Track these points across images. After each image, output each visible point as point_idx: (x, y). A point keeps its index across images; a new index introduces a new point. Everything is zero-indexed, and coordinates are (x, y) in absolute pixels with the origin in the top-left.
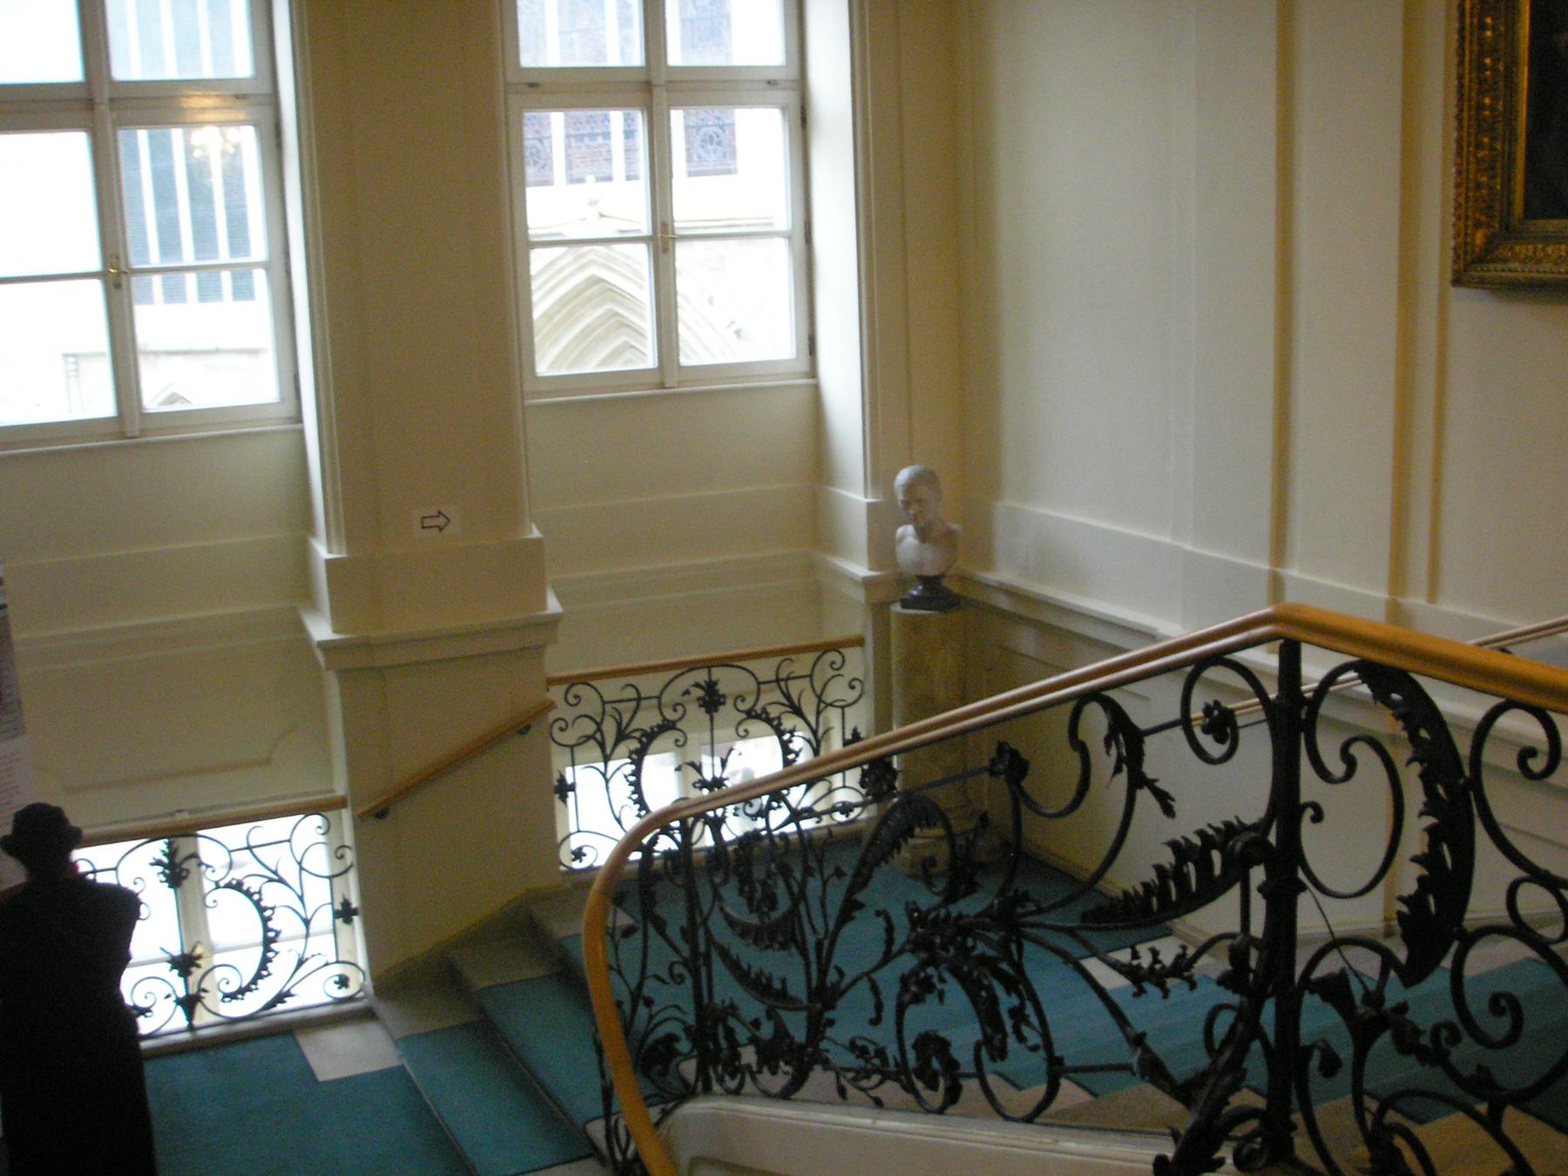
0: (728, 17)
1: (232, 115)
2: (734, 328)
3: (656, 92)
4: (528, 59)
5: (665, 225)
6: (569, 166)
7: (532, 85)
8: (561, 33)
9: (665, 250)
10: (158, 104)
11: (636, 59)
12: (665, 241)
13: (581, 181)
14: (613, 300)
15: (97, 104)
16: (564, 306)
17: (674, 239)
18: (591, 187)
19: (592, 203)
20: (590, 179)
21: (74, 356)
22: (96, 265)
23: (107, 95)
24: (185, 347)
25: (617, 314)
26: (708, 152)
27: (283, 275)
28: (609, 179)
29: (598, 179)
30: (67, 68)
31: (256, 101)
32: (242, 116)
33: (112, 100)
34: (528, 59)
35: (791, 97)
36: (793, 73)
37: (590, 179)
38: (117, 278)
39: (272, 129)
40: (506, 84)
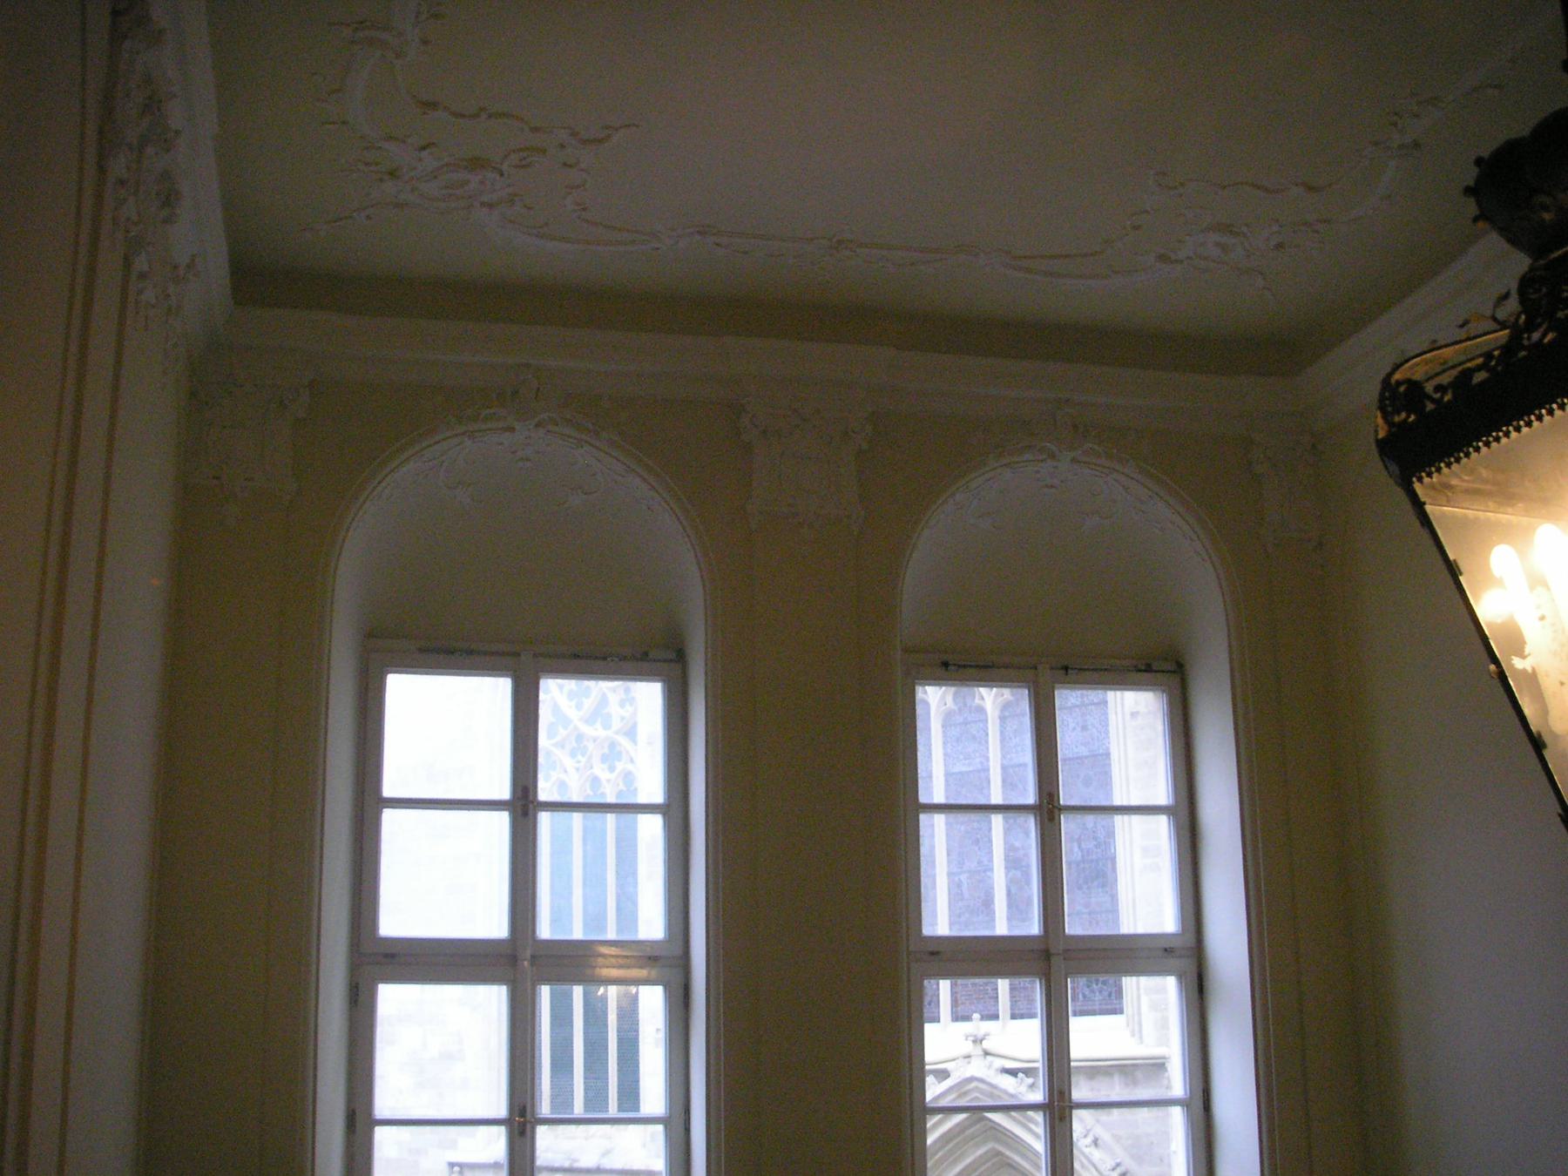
0: (1113, 860)
1: (643, 973)
2: (1119, 1170)
3: (1054, 960)
4: (927, 931)
5: (1061, 1093)
6: (955, 1002)
7: (932, 953)
8: (950, 874)
9: (1062, 1119)
10: (572, 962)
11: (1035, 928)
12: (1062, 1109)
13: (967, 1018)
14: (998, 1141)
15: (519, 962)
16: (948, 1142)
17: (1071, 1108)
18: (977, 1026)
19: (978, 1041)
20: (976, 1016)
21: (461, 1165)
22: (502, 1111)
23: (528, 953)
24: (567, 1164)
25: (999, 1153)
26: (1093, 991)
27: (681, 1130)
28: (995, 1017)
29: (982, 1018)
30: (493, 924)
31: (666, 963)
32: (654, 973)
33: (533, 957)
34: (927, 931)
35: (1189, 965)
36: (1190, 940)
37: (976, 1016)
38: (521, 1123)
39: (681, 991)
40: (909, 953)
